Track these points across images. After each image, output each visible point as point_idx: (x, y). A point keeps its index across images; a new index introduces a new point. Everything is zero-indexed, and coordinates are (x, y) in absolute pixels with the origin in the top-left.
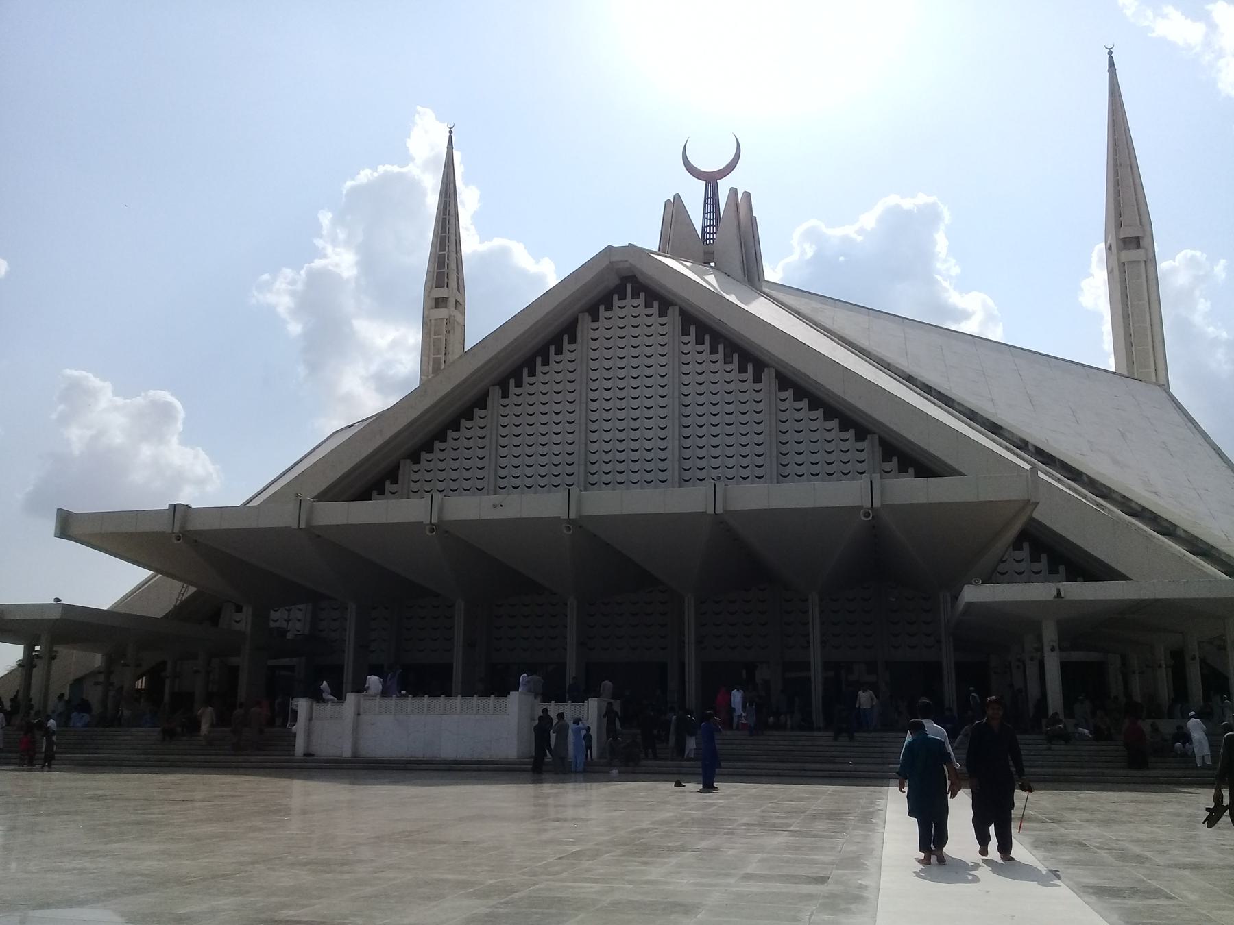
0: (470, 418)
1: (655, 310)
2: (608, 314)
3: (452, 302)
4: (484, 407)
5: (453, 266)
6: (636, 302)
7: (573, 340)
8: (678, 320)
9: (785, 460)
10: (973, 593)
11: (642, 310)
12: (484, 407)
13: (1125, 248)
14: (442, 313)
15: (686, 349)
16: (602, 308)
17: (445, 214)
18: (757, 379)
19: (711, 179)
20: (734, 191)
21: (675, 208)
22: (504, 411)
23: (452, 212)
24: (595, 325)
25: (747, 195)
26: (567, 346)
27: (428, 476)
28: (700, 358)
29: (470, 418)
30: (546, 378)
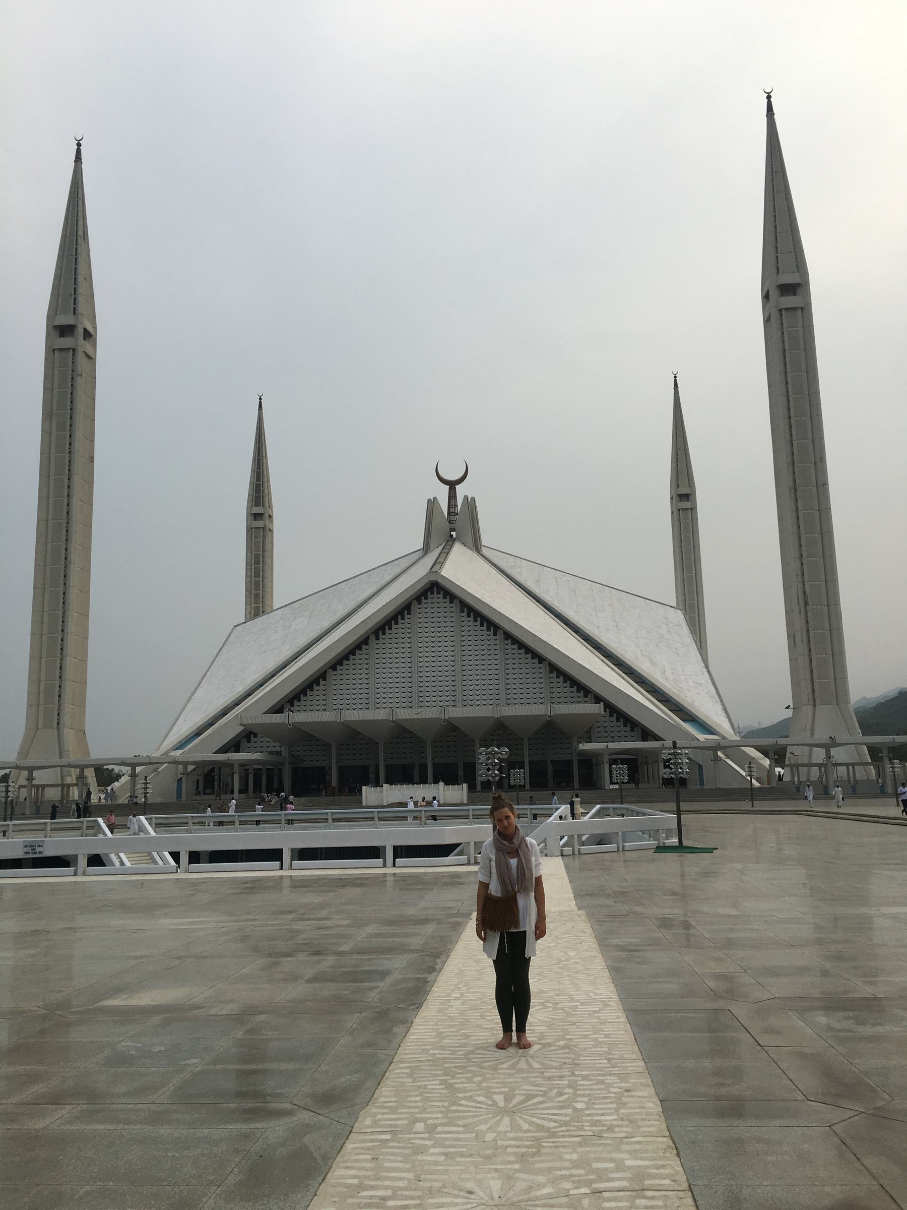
0: (361, 649)
1: (448, 600)
2: (426, 601)
4: (367, 644)
5: (266, 492)
7: (409, 613)
9: (508, 672)
10: (585, 746)
11: (441, 600)
12: (367, 644)
13: (680, 501)
14: (259, 524)
15: (462, 619)
17: (259, 455)
19: (452, 485)
20: (466, 497)
24: (420, 606)
25: (473, 499)
26: (406, 616)
27: (341, 677)
29: (361, 649)
30: (397, 631)
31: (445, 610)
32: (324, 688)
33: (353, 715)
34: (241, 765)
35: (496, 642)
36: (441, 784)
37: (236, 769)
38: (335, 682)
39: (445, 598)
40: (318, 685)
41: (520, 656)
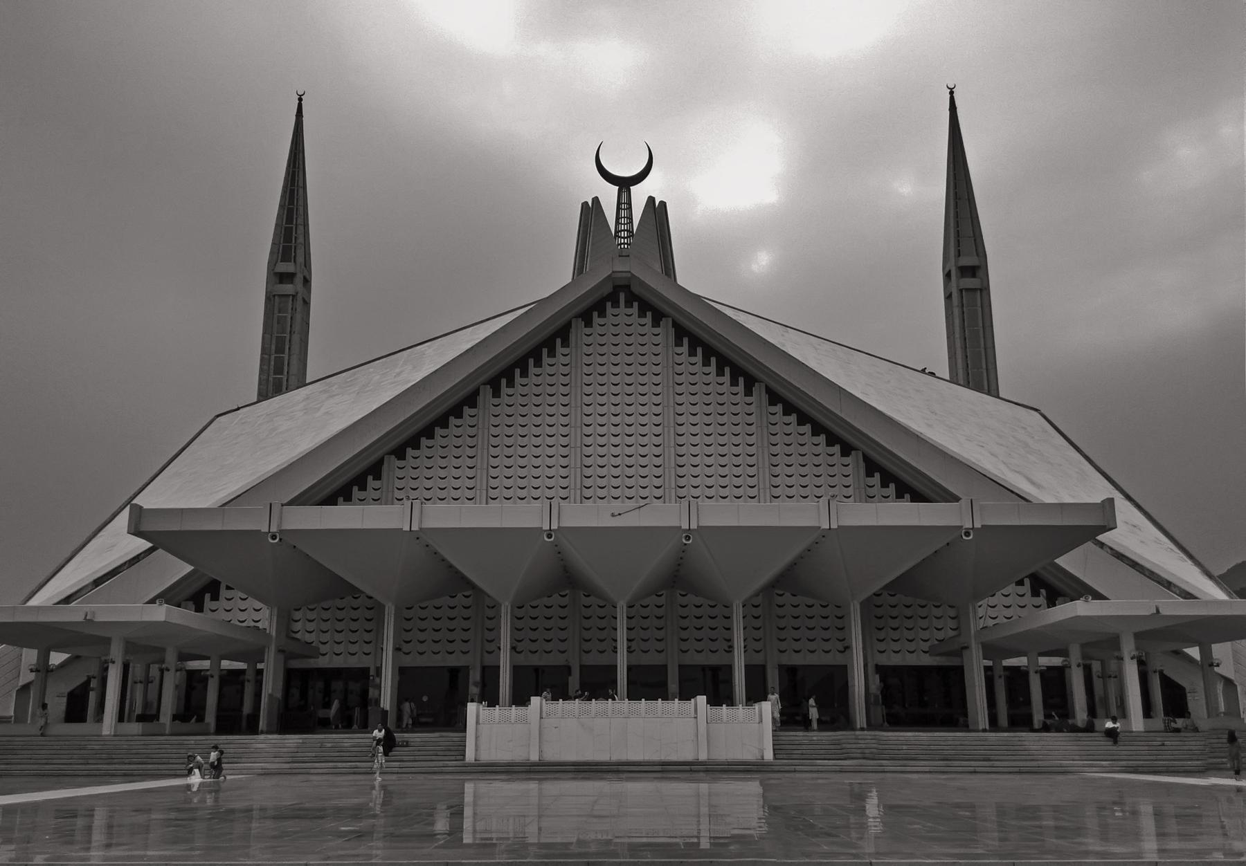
1: (648, 319)
2: (602, 321)
3: (299, 279)
5: (301, 240)
6: (629, 311)
7: (566, 343)
8: (672, 331)
11: (635, 318)
14: (288, 288)
15: (678, 359)
16: (595, 314)
17: (293, 185)
18: (748, 392)
19: (625, 184)
20: (651, 200)
21: (591, 211)
22: (497, 411)
23: (301, 184)
25: (663, 204)
26: (560, 350)
27: (414, 474)
28: (693, 369)
29: (459, 415)
31: (641, 340)
32: (376, 495)
33: (443, 516)
34: (131, 647)
35: (752, 409)
36: (702, 699)
37: (116, 652)
38: (399, 484)
39: (642, 314)
40: (363, 487)
41: (802, 440)
